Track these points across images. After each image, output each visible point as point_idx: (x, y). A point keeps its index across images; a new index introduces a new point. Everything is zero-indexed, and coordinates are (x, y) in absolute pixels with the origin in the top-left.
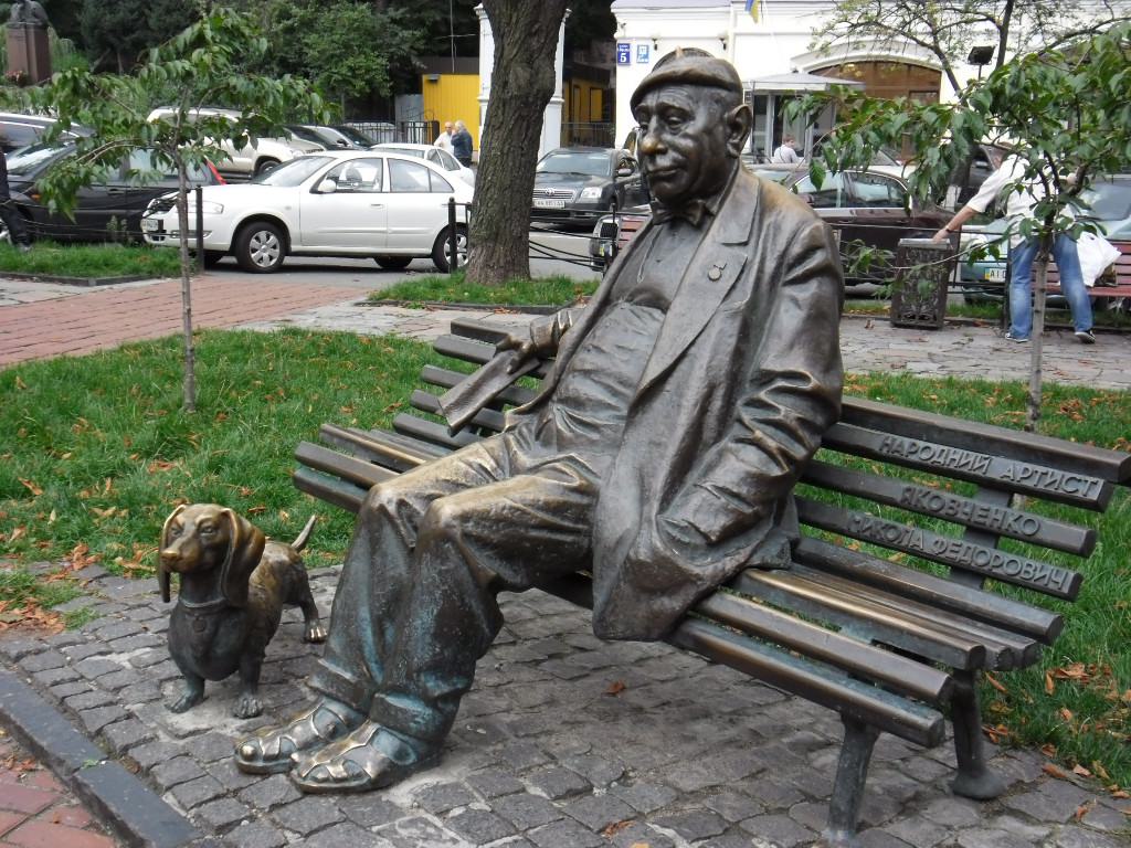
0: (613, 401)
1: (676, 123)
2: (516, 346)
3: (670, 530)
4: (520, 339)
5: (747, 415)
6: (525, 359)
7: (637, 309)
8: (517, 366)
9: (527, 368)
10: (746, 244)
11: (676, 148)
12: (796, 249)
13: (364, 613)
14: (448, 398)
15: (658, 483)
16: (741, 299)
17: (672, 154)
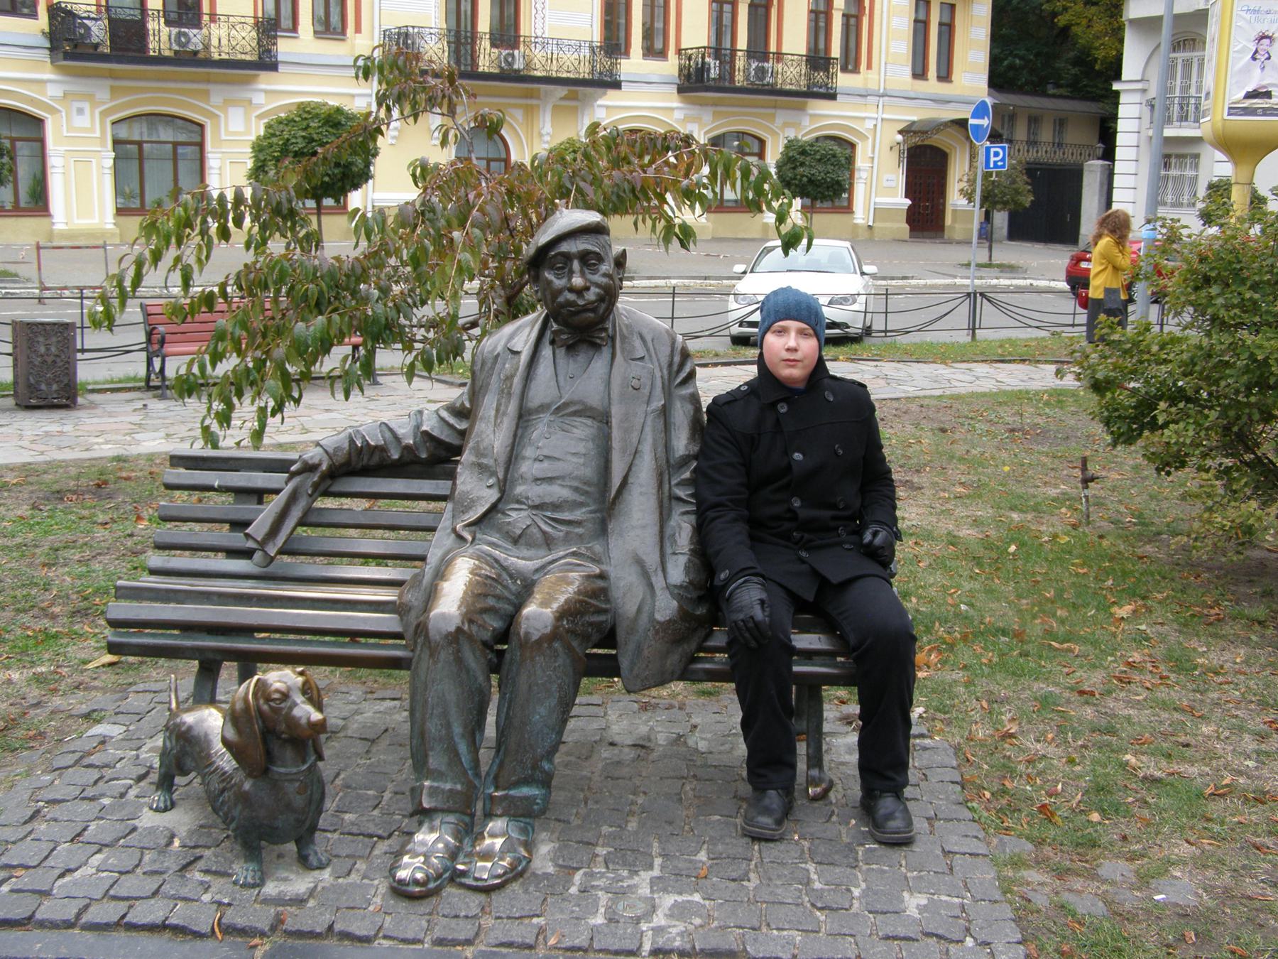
0: (582, 499)
2: (309, 468)
3: (676, 591)
4: (316, 461)
6: (323, 477)
7: (568, 420)
8: (316, 486)
9: (322, 488)
11: (598, 285)
12: (677, 359)
13: (457, 729)
14: (259, 528)
15: (652, 559)
16: (658, 403)
17: (594, 290)
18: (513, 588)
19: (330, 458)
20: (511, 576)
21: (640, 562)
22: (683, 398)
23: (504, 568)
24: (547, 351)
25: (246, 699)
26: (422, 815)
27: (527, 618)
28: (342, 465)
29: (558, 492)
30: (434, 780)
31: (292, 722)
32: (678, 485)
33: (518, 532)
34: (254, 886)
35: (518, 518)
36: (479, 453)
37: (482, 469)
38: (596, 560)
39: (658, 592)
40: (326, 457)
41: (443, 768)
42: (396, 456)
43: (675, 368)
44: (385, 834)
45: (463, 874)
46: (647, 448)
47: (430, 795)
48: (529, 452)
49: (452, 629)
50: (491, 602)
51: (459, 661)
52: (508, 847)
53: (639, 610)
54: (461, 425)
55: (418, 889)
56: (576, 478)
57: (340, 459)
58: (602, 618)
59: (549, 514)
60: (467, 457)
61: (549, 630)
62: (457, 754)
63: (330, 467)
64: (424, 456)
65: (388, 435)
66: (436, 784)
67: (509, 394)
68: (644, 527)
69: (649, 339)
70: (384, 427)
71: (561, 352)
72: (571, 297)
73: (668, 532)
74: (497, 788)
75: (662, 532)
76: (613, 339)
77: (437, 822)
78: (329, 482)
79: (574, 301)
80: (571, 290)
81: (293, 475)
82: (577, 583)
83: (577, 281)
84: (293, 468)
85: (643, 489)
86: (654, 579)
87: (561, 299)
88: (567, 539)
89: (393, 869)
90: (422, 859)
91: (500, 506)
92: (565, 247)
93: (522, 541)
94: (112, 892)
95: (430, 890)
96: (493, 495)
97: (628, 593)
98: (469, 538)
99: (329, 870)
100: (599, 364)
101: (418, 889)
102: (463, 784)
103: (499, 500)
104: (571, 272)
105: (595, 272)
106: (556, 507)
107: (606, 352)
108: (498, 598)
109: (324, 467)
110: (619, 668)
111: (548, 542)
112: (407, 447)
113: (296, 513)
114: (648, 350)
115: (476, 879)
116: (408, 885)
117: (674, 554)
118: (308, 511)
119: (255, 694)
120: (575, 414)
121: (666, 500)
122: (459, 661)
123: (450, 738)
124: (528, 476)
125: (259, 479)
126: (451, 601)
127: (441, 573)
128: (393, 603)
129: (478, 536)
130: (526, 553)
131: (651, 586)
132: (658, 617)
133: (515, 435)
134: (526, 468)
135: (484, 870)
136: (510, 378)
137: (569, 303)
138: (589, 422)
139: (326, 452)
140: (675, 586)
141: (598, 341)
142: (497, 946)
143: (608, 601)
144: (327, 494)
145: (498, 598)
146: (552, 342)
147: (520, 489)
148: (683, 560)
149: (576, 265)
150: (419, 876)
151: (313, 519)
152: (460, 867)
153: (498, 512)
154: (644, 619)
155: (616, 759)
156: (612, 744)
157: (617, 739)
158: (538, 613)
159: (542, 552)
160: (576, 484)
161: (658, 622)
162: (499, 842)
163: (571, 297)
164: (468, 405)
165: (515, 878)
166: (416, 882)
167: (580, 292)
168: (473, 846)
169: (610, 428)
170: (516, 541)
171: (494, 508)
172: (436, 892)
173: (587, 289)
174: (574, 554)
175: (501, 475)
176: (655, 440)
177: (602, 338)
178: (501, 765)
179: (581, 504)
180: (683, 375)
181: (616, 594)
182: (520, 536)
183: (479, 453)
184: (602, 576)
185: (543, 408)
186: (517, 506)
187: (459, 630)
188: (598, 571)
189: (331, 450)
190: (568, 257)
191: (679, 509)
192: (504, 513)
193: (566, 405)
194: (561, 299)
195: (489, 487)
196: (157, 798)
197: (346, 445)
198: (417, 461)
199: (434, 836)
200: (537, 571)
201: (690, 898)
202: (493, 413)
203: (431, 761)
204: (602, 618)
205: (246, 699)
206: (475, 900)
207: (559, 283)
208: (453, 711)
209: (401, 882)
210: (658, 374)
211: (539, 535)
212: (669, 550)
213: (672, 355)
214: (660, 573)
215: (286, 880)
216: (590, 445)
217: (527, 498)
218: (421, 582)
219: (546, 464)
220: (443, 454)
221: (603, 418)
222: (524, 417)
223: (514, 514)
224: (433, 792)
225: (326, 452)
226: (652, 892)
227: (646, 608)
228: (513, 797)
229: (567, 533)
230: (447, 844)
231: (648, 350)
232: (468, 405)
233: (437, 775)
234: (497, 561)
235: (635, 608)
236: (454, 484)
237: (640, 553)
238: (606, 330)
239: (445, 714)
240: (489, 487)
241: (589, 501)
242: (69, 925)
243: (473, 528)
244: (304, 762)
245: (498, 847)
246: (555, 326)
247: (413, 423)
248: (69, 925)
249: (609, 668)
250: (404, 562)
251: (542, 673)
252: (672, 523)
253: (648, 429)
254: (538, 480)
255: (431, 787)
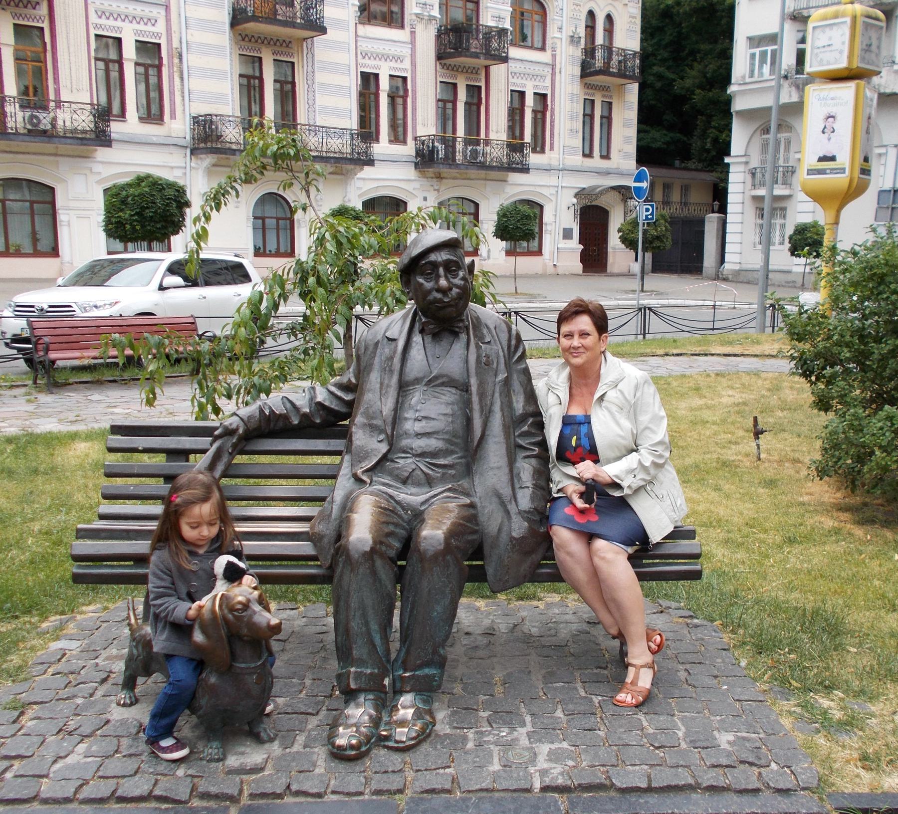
1: (455, 271)
2: (229, 432)
3: (526, 515)
4: (234, 426)
5: (520, 441)
7: (438, 389)
8: (234, 446)
9: (239, 448)
10: (489, 343)
11: (457, 286)
12: (513, 342)
13: (374, 627)
15: (506, 491)
16: (502, 376)
17: (455, 291)
18: (406, 517)
19: (245, 424)
20: (403, 508)
21: (499, 496)
22: (519, 372)
23: (398, 502)
24: (417, 338)
25: (213, 611)
26: (350, 695)
27: (425, 538)
28: (255, 429)
29: (433, 444)
30: (357, 667)
31: (253, 626)
32: (519, 436)
33: (406, 474)
34: (218, 760)
35: (405, 464)
36: (369, 416)
37: (373, 428)
38: (468, 495)
39: (514, 516)
40: (242, 424)
41: (365, 657)
42: (296, 422)
43: (512, 349)
44: (314, 712)
45: (387, 738)
46: (497, 407)
47: (356, 679)
48: (409, 414)
49: (368, 549)
50: (391, 528)
51: (374, 573)
52: (418, 715)
53: (500, 530)
54: (348, 397)
55: (353, 753)
56: (446, 433)
57: (252, 426)
58: (475, 537)
59: (428, 460)
60: (359, 419)
61: (442, 547)
62: (374, 646)
63: (245, 431)
64: (318, 421)
65: (288, 405)
66: (359, 670)
67: (391, 371)
68: (499, 468)
69: (492, 327)
70: (285, 399)
71: (428, 339)
72: (439, 296)
73: (515, 471)
74: (405, 671)
75: (511, 471)
76: (467, 328)
77: (361, 699)
78: (244, 443)
79: (440, 299)
80: (439, 290)
81: (216, 438)
82: (456, 511)
83: (443, 282)
84: (216, 433)
85: (496, 440)
86: (509, 507)
87: (431, 297)
88: (443, 479)
89: (331, 737)
90: (355, 729)
91: (389, 456)
92: (433, 257)
93: (410, 481)
94: (100, 774)
95: (363, 752)
96: (384, 448)
97: (492, 519)
98: (368, 481)
99: (277, 742)
100: (458, 347)
101: (353, 753)
102: (379, 669)
103: (389, 451)
104: (438, 277)
105: (456, 276)
106: (434, 454)
107: (463, 336)
108: (396, 525)
109: (241, 431)
110: (486, 575)
111: (429, 482)
112: (305, 415)
113: (220, 468)
114: (493, 337)
115: (397, 742)
116: (345, 750)
117: (521, 488)
118: (229, 465)
119: (220, 606)
120: (442, 384)
121: (513, 447)
122: (374, 573)
123: (369, 633)
124: (412, 432)
125: (186, 442)
126: (362, 531)
127: (348, 506)
128: (307, 533)
129: (375, 479)
130: (414, 490)
131: (507, 512)
132: (514, 534)
133: (397, 402)
134: (409, 426)
135: (402, 734)
136: (391, 358)
137: (436, 301)
138: (453, 390)
139: (242, 419)
140: (525, 511)
141: (457, 330)
142: (422, 792)
143: (477, 524)
144: (243, 452)
145: (396, 525)
146: (422, 331)
147: (405, 442)
148: (528, 492)
149: (441, 270)
150: (354, 742)
151: (232, 472)
152: (384, 733)
153: (388, 460)
154: (504, 537)
155: (473, 645)
156: (467, 634)
157: (470, 630)
158: (433, 534)
159: (426, 489)
160: (446, 437)
161: (514, 538)
162: (411, 712)
163: (439, 296)
164: (354, 381)
165: (424, 740)
166: (352, 747)
167: (444, 291)
168: (390, 716)
169: (471, 394)
170: (404, 482)
171: (385, 458)
172: (368, 752)
173: (451, 289)
174: (449, 490)
175: (389, 432)
176: (502, 402)
177: (458, 327)
178: (408, 652)
179: (452, 452)
180: (518, 354)
181: (482, 519)
182: (408, 478)
183: (369, 416)
184: (472, 506)
185: (417, 381)
186: (403, 455)
187: (373, 549)
188: (469, 501)
189: (245, 419)
190: (435, 265)
191: (522, 454)
192: (393, 461)
193: (436, 378)
194: (431, 297)
195: (379, 442)
196: (123, 696)
197: (257, 414)
198: (313, 425)
199: (361, 710)
200: (423, 503)
201: (560, 746)
202: (378, 386)
203: (354, 652)
204: (475, 537)
205: (213, 611)
206: (397, 758)
207: (428, 285)
208: (370, 613)
209: (340, 747)
210: (501, 354)
211: (422, 476)
212: (517, 486)
213: (509, 340)
214: (513, 502)
215: (243, 753)
216: (456, 407)
217: (412, 449)
218: (330, 515)
219: (424, 423)
220: (333, 419)
221: (465, 388)
222: (404, 387)
223: (401, 461)
224: (358, 675)
225: (242, 419)
226: (531, 743)
227: (505, 528)
228: (418, 676)
229: (444, 474)
230: (371, 717)
231: (493, 337)
232: (354, 381)
233: (360, 663)
234: (391, 497)
235: (496, 529)
236: (351, 441)
237: (498, 487)
238: (462, 321)
239: (364, 616)
240: (379, 442)
241: (457, 450)
242: (67, 800)
243: (370, 473)
244: (260, 658)
245: (410, 717)
246: (424, 320)
247: (307, 397)
248: (67, 800)
249: (478, 576)
250: (310, 503)
251: (433, 581)
252: (518, 465)
253: (497, 395)
254: (419, 435)
255: (356, 672)
